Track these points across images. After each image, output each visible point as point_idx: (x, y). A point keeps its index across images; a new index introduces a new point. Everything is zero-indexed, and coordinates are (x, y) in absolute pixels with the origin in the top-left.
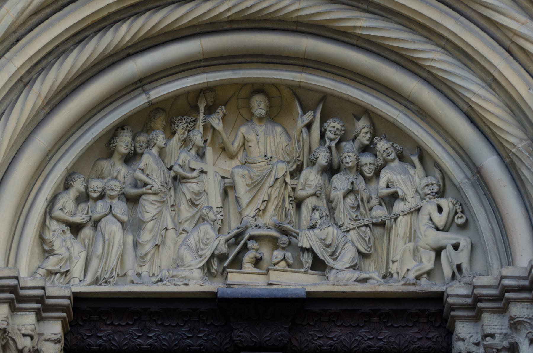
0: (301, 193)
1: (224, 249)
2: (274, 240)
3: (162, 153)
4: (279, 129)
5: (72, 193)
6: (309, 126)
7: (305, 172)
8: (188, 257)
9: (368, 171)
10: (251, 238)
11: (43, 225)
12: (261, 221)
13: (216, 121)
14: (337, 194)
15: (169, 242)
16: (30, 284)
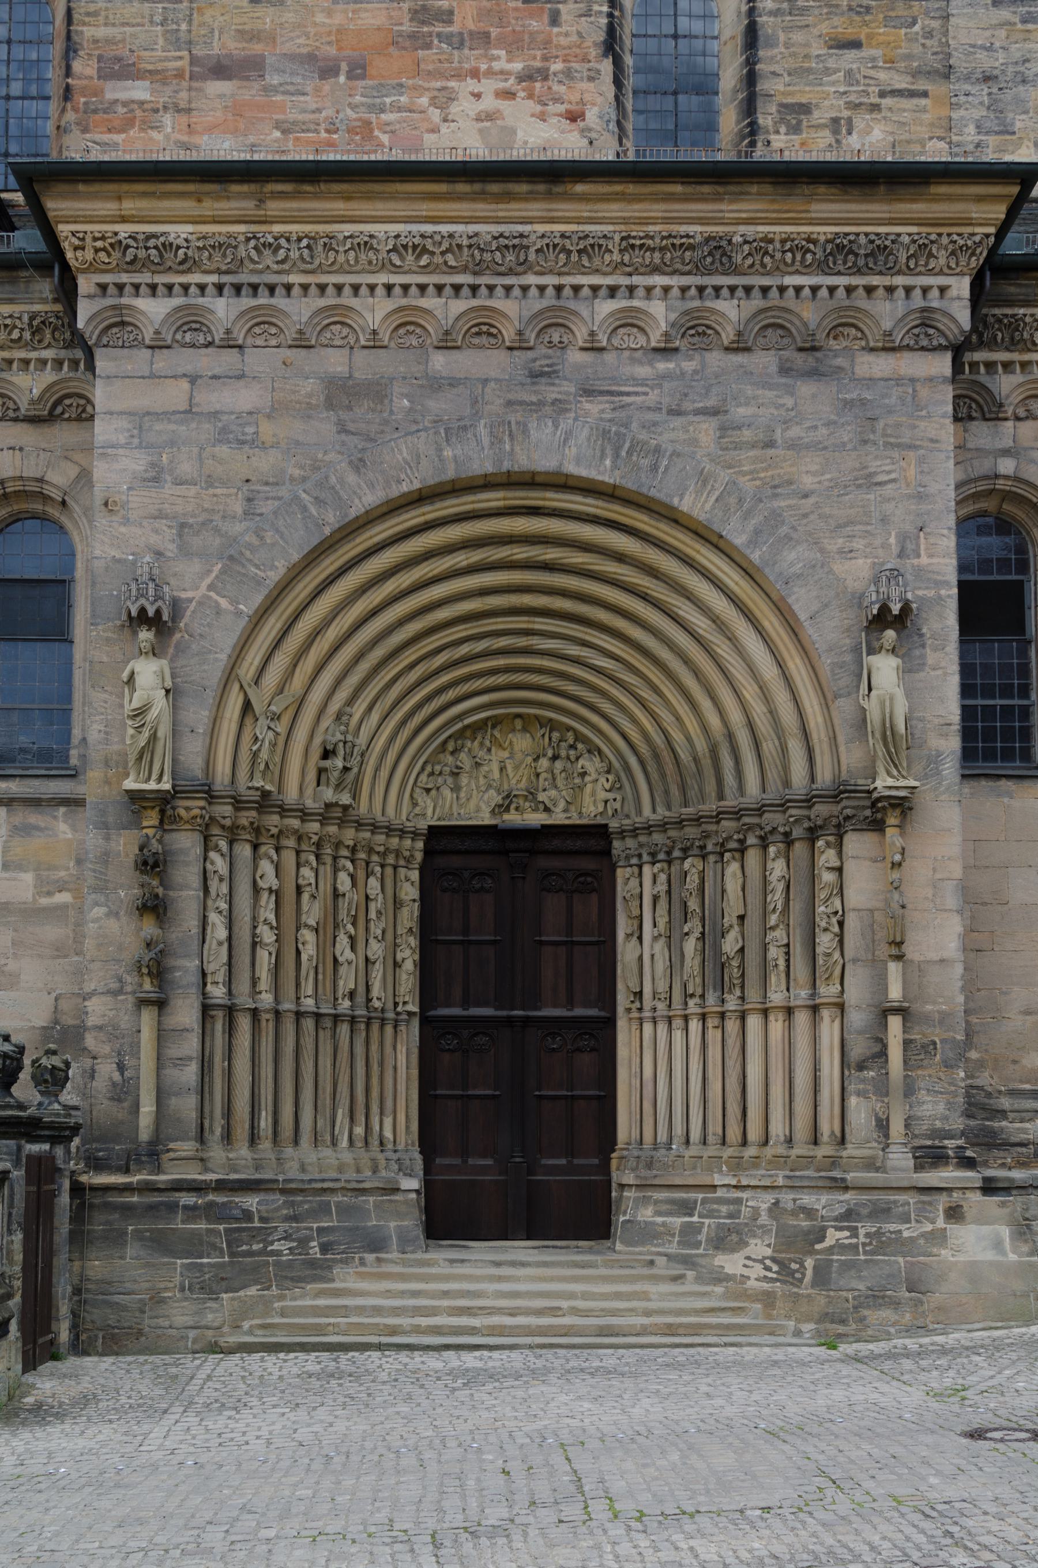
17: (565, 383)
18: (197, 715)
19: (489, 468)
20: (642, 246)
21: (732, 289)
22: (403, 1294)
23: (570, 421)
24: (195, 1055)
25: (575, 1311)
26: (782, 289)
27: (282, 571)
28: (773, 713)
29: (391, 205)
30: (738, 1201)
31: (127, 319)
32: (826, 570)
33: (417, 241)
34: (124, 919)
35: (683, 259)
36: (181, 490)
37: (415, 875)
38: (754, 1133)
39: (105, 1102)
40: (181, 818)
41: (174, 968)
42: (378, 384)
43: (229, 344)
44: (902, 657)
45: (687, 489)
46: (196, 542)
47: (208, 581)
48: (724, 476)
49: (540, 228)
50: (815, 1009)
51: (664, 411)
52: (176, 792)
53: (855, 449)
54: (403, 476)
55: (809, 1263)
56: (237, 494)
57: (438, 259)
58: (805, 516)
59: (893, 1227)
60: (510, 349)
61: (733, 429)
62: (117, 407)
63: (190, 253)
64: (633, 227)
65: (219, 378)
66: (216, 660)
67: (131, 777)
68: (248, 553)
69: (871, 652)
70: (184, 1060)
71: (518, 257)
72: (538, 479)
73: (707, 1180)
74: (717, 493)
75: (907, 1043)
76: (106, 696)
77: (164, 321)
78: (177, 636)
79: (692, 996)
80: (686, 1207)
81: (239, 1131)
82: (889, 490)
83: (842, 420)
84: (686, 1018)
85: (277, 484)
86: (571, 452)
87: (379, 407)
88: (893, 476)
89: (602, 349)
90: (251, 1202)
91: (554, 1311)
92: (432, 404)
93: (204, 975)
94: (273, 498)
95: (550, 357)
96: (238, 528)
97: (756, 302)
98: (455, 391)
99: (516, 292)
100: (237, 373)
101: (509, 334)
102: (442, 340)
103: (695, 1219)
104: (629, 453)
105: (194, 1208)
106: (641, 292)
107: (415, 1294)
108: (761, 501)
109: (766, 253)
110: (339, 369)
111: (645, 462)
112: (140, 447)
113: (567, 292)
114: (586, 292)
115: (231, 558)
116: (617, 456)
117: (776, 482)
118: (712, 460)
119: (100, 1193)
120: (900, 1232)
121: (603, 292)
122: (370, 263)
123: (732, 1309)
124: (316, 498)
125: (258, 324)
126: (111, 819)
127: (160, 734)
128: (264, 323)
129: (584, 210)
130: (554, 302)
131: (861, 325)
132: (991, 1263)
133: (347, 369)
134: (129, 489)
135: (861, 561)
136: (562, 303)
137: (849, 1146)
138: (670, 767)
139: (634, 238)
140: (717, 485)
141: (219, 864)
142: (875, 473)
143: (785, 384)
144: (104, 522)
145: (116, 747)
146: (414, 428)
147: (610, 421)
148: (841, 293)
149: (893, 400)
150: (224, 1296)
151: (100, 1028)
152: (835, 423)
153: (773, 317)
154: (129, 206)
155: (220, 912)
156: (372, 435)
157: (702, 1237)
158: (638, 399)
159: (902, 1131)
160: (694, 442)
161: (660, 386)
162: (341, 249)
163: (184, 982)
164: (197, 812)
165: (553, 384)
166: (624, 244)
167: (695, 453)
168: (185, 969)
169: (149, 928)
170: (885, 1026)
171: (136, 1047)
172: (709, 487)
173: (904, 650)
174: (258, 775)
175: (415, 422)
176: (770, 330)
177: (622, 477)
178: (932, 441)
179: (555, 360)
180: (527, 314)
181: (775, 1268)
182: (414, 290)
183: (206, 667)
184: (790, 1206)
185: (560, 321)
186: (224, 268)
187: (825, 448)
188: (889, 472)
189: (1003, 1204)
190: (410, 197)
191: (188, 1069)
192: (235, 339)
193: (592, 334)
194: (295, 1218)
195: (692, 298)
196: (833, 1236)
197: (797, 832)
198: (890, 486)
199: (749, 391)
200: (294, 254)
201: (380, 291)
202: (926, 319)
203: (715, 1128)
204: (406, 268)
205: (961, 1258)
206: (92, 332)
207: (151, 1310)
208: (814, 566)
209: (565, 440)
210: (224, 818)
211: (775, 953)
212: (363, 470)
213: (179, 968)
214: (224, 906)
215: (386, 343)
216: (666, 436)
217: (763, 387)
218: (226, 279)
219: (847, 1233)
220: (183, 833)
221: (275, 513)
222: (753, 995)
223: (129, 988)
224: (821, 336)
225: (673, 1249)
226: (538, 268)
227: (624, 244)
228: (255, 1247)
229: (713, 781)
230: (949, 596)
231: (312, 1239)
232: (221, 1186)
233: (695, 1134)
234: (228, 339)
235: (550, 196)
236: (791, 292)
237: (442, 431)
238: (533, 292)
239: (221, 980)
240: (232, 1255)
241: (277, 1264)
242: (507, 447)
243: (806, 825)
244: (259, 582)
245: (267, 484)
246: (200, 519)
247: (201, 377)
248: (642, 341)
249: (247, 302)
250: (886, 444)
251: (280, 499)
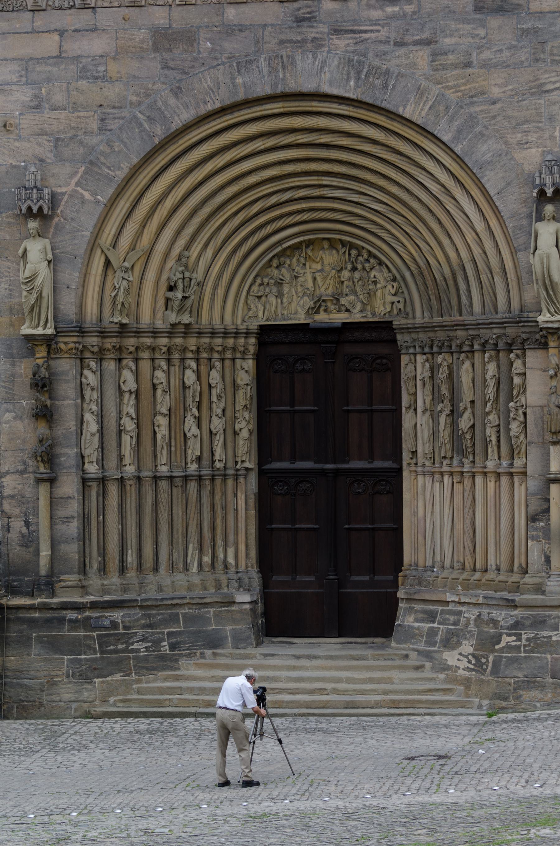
0: (343, 279)
1: (313, 306)
2: (332, 300)
3: (289, 266)
4: (334, 252)
5: (257, 284)
6: (345, 252)
7: (343, 272)
8: (300, 310)
9: (368, 269)
10: (324, 301)
11: (247, 298)
12: (327, 292)
13: (309, 252)
14: (356, 280)
15: (294, 300)
16: (242, 327)
17: (321, 25)
24: (76, 515)
25: (336, 691)
27: (126, 171)
32: (509, 157)
34: (26, 421)
36: (56, 113)
37: (250, 364)
39: (17, 547)
40: (62, 350)
41: (61, 455)
45: (408, 101)
47: (76, 179)
48: (435, 90)
51: (392, 43)
52: (57, 332)
53: (530, 66)
54: (208, 99)
56: (94, 116)
58: (494, 117)
61: (441, 54)
65: (80, 31)
66: (83, 236)
67: (27, 324)
68: (102, 158)
70: (68, 519)
74: (430, 103)
76: (9, 264)
78: (56, 220)
83: (521, 44)
85: (121, 108)
86: (326, 76)
87: (190, 49)
90: (118, 615)
91: (321, 691)
92: (227, 45)
94: (119, 118)
95: (310, 7)
96: (95, 140)
98: (243, 34)
100: (91, 27)
105: (76, 621)
108: (462, 107)
110: (162, 22)
111: (378, 82)
112: (26, 84)
115: (91, 162)
116: (358, 78)
117: (473, 93)
118: (427, 79)
119: (14, 611)
123: (444, 690)
124: (148, 117)
133: (167, 21)
134: (21, 114)
135: (534, 150)
140: (430, 97)
141: (91, 378)
142: (545, 84)
143: (479, 19)
144: (4, 139)
145: (16, 300)
147: (354, 52)
150: (97, 680)
151: (12, 497)
152: (515, 47)
155: (92, 413)
156: (186, 69)
158: (373, 35)
160: (413, 65)
161: (388, 24)
164: (72, 345)
165: (312, 27)
167: (414, 73)
169: (42, 428)
171: (36, 509)
172: (425, 99)
175: (216, 59)
177: (362, 94)
179: (313, 9)
181: (474, 662)
183: (76, 242)
184: (485, 618)
187: (508, 66)
188: (555, 82)
191: (71, 524)
199: (453, 25)
207: (48, 689)
208: (500, 155)
209: (322, 68)
210: (93, 346)
212: (180, 95)
216: (394, 62)
217: (463, 23)
220: (64, 360)
221: (120, 129)
223: (31, 469)
228: (120, 647)
234: (84, 4)
237: (235, 64)
240: (102, 652)
241: (135, 658)
242: (281, 75)
244: (110, 179)
245: (114, 107)
246: (69, 135)
247: (67, 31)
250: (553, 61)
251: (123, 118)
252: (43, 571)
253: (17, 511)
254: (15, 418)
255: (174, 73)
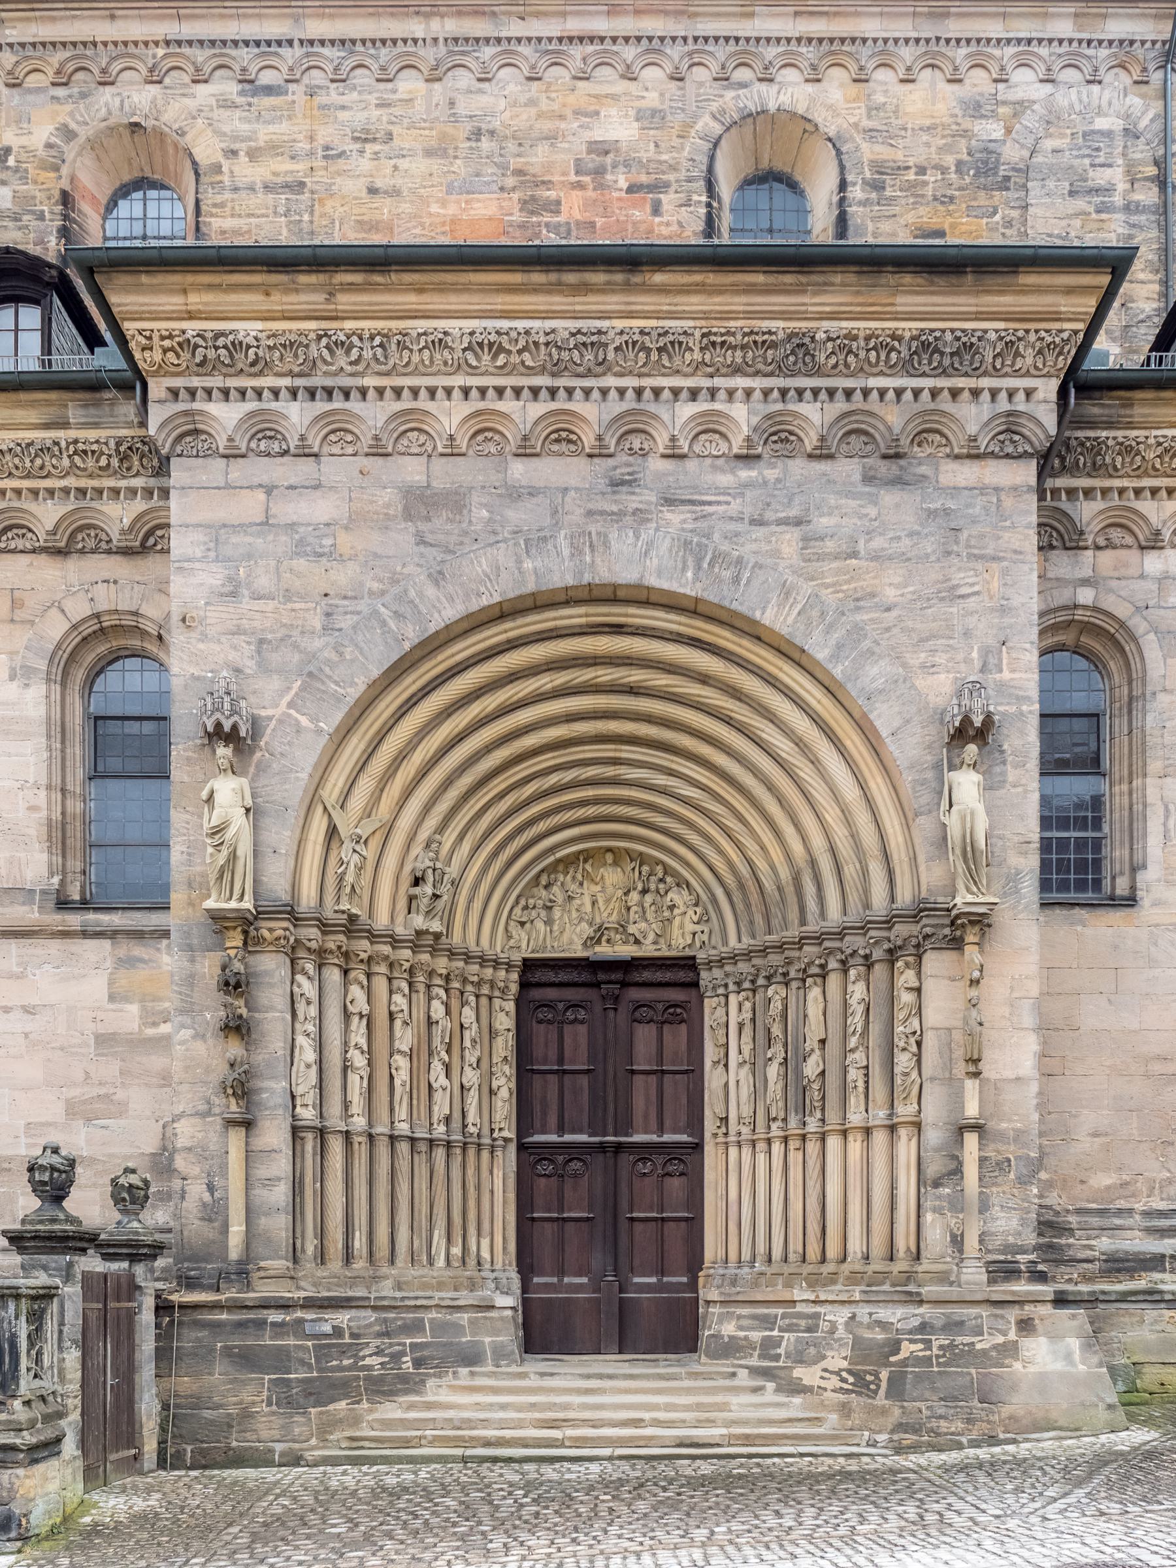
18: (281, 835)
19: (570, 581)
20: (723, 343)
21: (816, 392)
22: (490, 1407)
23: (652, 532)
25: (657, 1423)
26: (866, 392)
27: (362, 688)
28: (854, 836)
29: (465, 298)
30: (816, 1316)
31: (200, 426)
32: (908, 684)
33: (493, 338)
34: (211, 1041)
35: (765, 358)
38: (833, 1251)
39: (197, 1222)
42: (457, 493)
43: (306, 453)
44: (983, 774)
46: (275, 658)
47: (288, 698)
48: (807, 588)
49: (619, 324)
50: (892, 1129)
51: (746, 521)
54: (483, 589)
55: (884, 1375)
57: (515, 359)
58: (888, 629)
59: (967, 1340)
60: (590, 456)
62: (193, 519)
63: (261, 354)
64: (714, 323)
66: (297, 779)
68: (327, 670)
69: (952, 767)
70: (271, 1181)
71: (596, 357)
72: (621, 594)
73: (787, 1296)
74: (799, 607)
75: (982, 1160)
76: (188, 817)
77: (237, 427)
78: (258, 755)
79: (775, 1119)
80: (768, 1322)
81: (332, 1250)
82: (972, 603)
84: (769, 1141)
86: (653, 563)
88: (976, 588)
89: (683, 457)
90: (343, 1318)
91: (637, 1423)
92: (511, 514)
93: (293, 1097)
94: (352, 613)
95: (629, 465)
96: (318, 643)
97: (839, 405)
98: (534, 500)
99: (595, 394)
100: (313, 483)
101: (588, 441)
102: (520, 447)
103: (775, 1333)
104: (711, 564)
106: (722, 395)
107: (503, 1407)
108: (843, 614)
109: (850, 352)
110: (417, 478)
111: (727, 574)
112: (217, 560)
113: (648, 394)
114: (666, 394)
115: (310, 674)
116: (698, 567)
117: (859, 595)
120: (973, 1344)
121: (684, 395)
122: (446, 363)
123: (809, 1419)
125: (333, 432)
126: (195, 941)
127: (240, 853)
128: (340, 430)
129: (663, 303)
130: (634, 405)
131: (946, 431)
132: (1062, 1375)
133: (425, 478)
134: (207, 604)
135: (943, 676)
136: (641, 406)
137: (923, 1261)
138: (754, 897)
139: (715, 334)
142: (958, 586)
143: (869, 493)
144: (182, 638)
145: (199, 869)
146: (493, 539)
148: (926, 395)
149: (977, 510)
151: (190, 1149)
152: (918, 533)
153: (857, 422)
154: (195, 300)
157: (781, 1351)
158: (721, 509)
159: (977, 1246)
160: (776, 554)
161: (742, 495)
162: (415, 348)
163: (271, 1104)
165: (633, 493)
166: (705, 341)
168: (272, 1091)
170: (960, 1142)
173: (985, 767)
174: (344, 898)
175: (495, 533)
176: (853, 436)
178: (1015, 552)
180: (607, 418)
181: (851, 1380)
182: (491, 393)
184: (866, 1319)
185: (641, 426)
186: (296, 369)
187: (909, 559)
188: (973, 585)
189: (1074, 1316)
190: (485, 289)
192: (310, 447)
193: (673, 439)
194: (387, 1334)
195: (775, 401)
196: (908, 1349)
197: (878, 954)
198: (973, 599)
199: (832, 500)
200: (368, 354)
201: (457, 394)
202: (1011, 425)
203: (795, 1245)
204: (483, 369)
205: (1032, 1369)
206: (165, 440)
211: (853, 1074)
212: (442, 583)
213: (266, 1090)
214: (310, 1028)
215: (464, 450)
218: (300, 382)
219: (921, 1346)
221: (354, 628)
222: (833, 1117)
224: (905, 441)
225: (754, 1361)
226: (617, 369)
227: (705, 341)
229: (796, 908)
230: (1030, 712)
231: (404, 1354)
232: (309, 1304)
233: (777, 1253)
234: (304, 447)
235: (628, 287)
236: (875, 394)
238: (613, 394)
239: (310, 1102)
242: (588, 559)
243: (886, 946)
244: (339, 699)
245: (345, 598)
246: (279, 635)
247: (276, 487)
248: (724, 447)
249: (321, 406)
250: (970, 555)
251: (358, 613)
252: (234, 1254)
253: (196, 1170)
254: (194, 1037)
255: (434, 551)
